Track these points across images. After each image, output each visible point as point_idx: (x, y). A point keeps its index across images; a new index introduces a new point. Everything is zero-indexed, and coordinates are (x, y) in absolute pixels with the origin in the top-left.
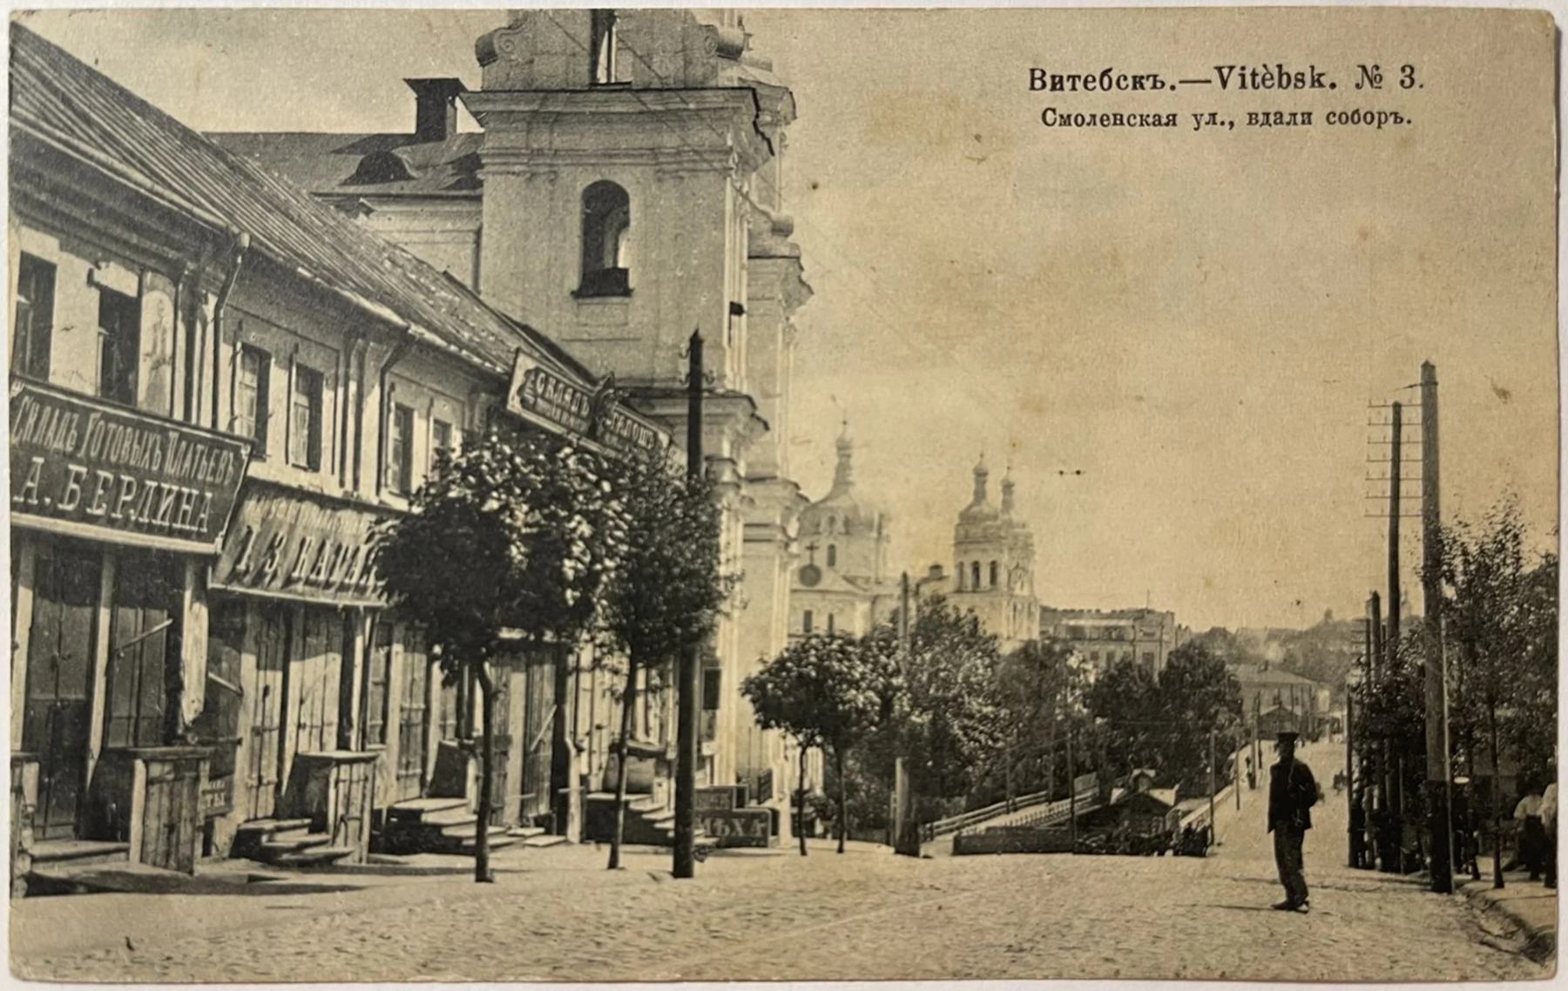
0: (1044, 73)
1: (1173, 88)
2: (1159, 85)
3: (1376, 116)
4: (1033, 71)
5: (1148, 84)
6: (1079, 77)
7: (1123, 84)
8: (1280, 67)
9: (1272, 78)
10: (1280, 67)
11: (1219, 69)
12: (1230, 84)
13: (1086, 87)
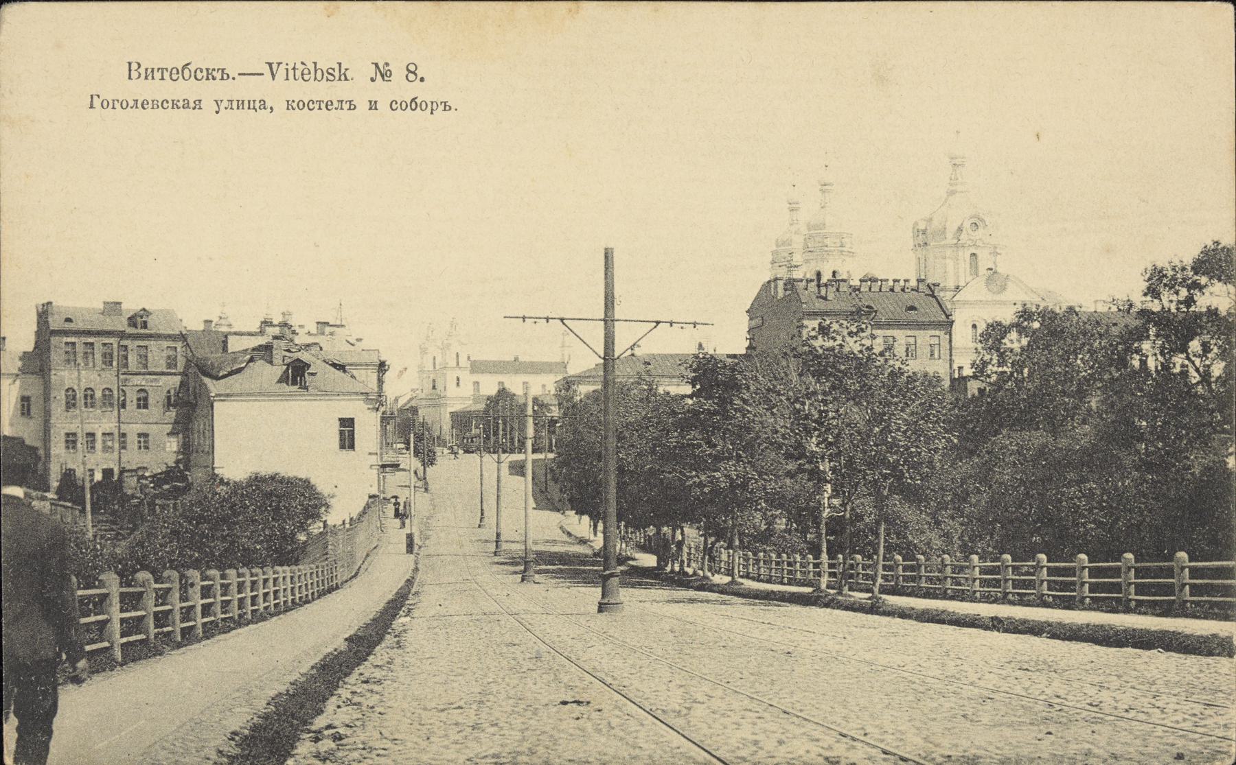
1: (234, 79)
2: (225, 77)
3: (429, 104)
4: (130, 64)
5: (218, 75)
6: (167, 69)
7: (199, 75)
8: (315, 63)
9: (310, 73)
10: (315, 63)
11: (270, 64)
12: (276, 78)
13: (171, 79)
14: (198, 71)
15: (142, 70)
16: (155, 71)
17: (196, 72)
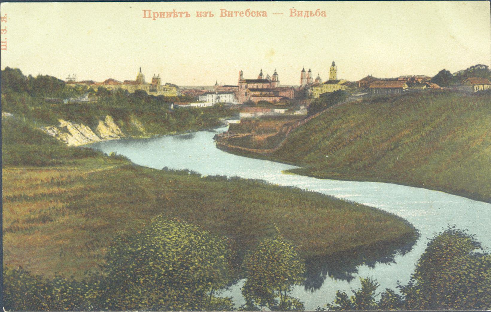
0: (226, 11)
6: (238, 12)
7: (254, 14)
14: (253, 13)
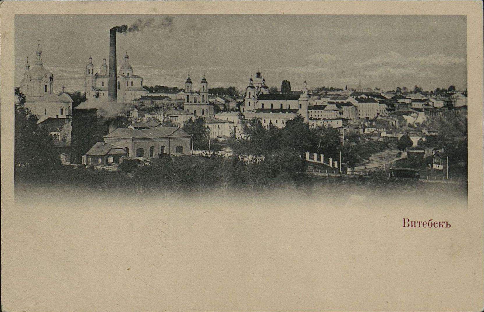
2: (448, 226)
4: (404, 219)
5: (445, 225)
7: (436, 225)
13: (423, 226)
14: (436, 223)
15: (410, 223)
16: (416, 223)
17: (434, 223)
